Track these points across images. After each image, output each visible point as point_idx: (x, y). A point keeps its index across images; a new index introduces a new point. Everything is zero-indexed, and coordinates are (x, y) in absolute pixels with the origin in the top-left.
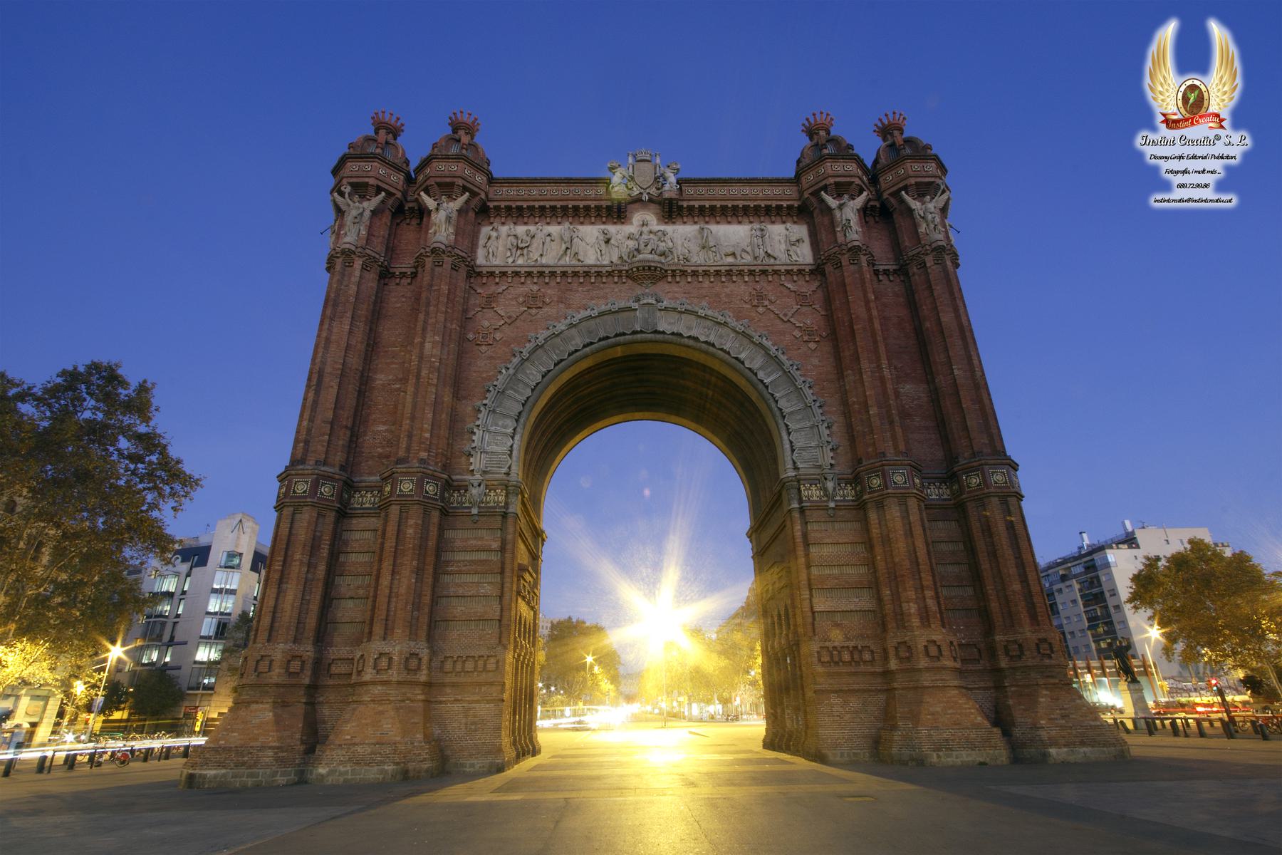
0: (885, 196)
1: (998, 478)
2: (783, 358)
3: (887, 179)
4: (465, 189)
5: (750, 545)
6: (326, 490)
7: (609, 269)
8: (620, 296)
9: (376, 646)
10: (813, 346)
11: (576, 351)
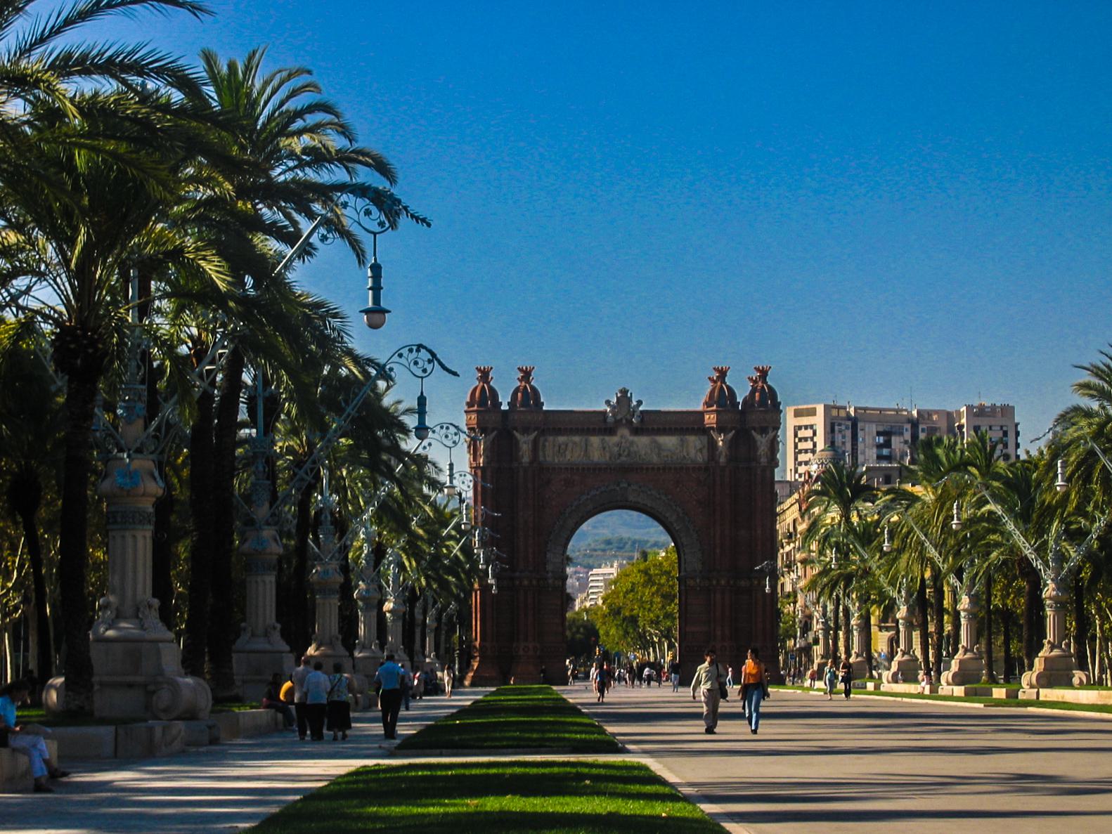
10: (700, 510)
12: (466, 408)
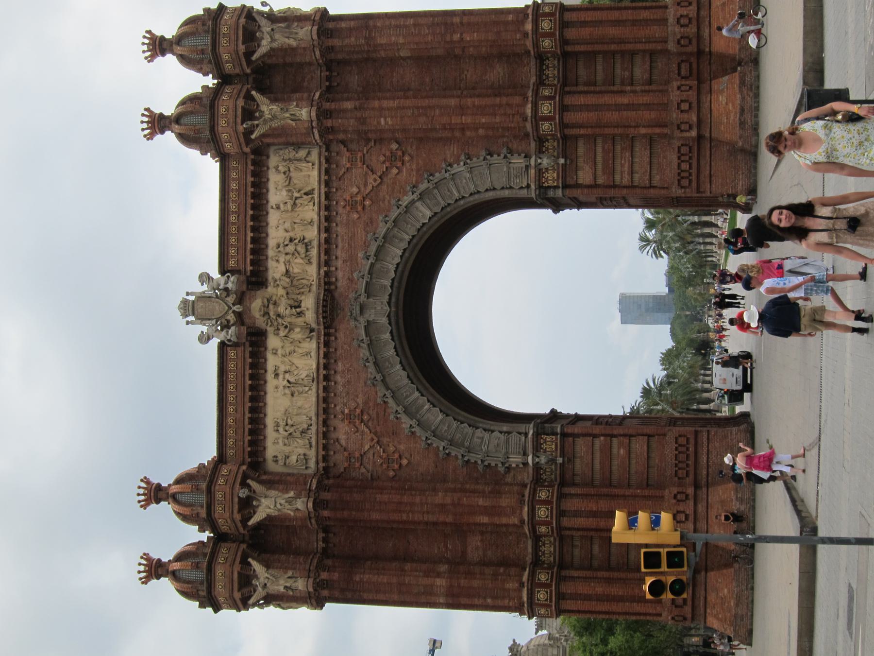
0: (248, 71)
1: (546, 25)
3: (228, 67)
5: (567, 211)
6: (543, 577)
7: (322, 346)
10: (407, 158)
11: (408, 377)
12: (210, 610)
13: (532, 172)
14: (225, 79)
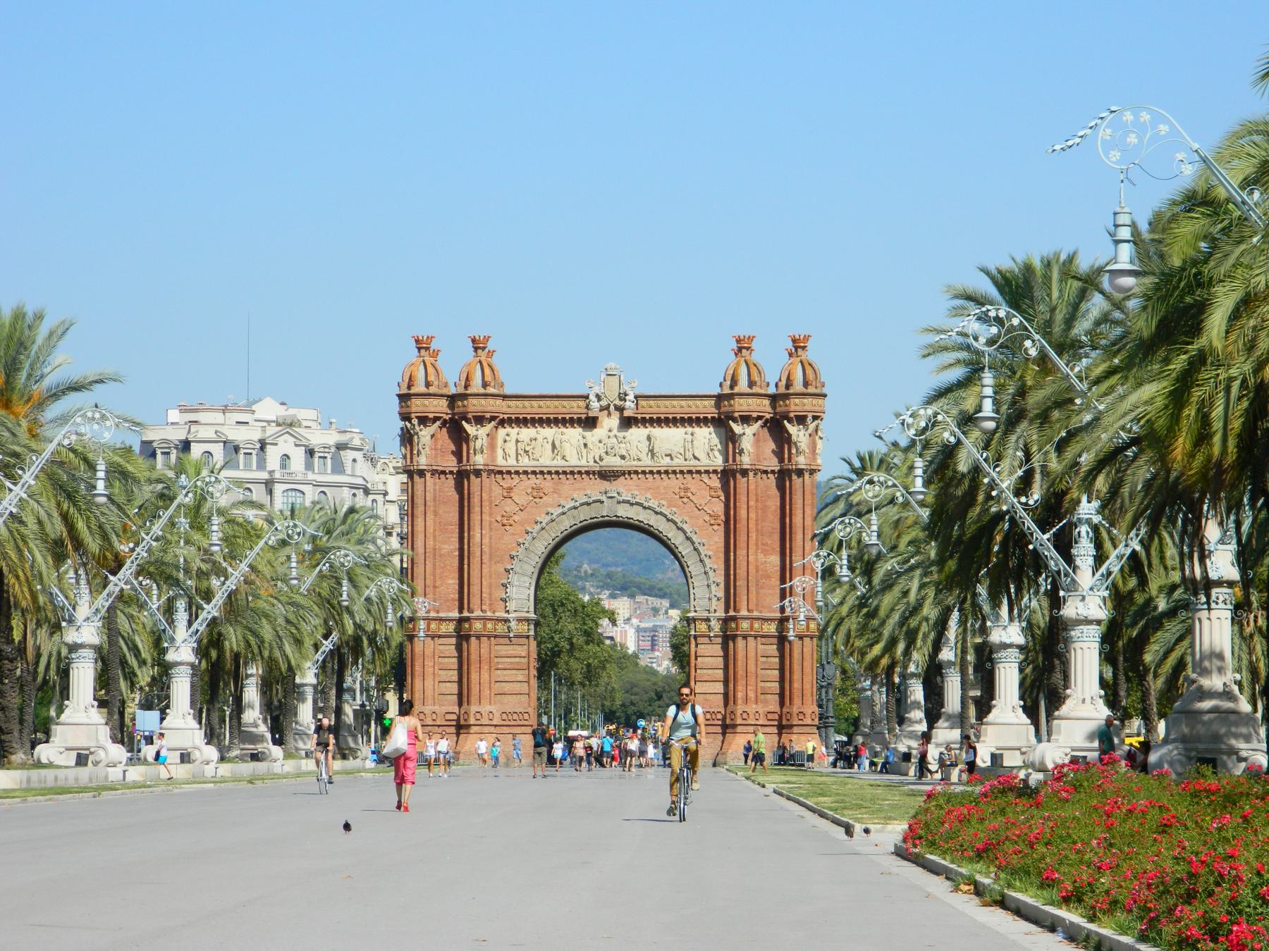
2: (695, 538)
4: (493, 418)
8: (595, 488)
9: (474, 708)
13: (706, 614)
14: (774, 399)
